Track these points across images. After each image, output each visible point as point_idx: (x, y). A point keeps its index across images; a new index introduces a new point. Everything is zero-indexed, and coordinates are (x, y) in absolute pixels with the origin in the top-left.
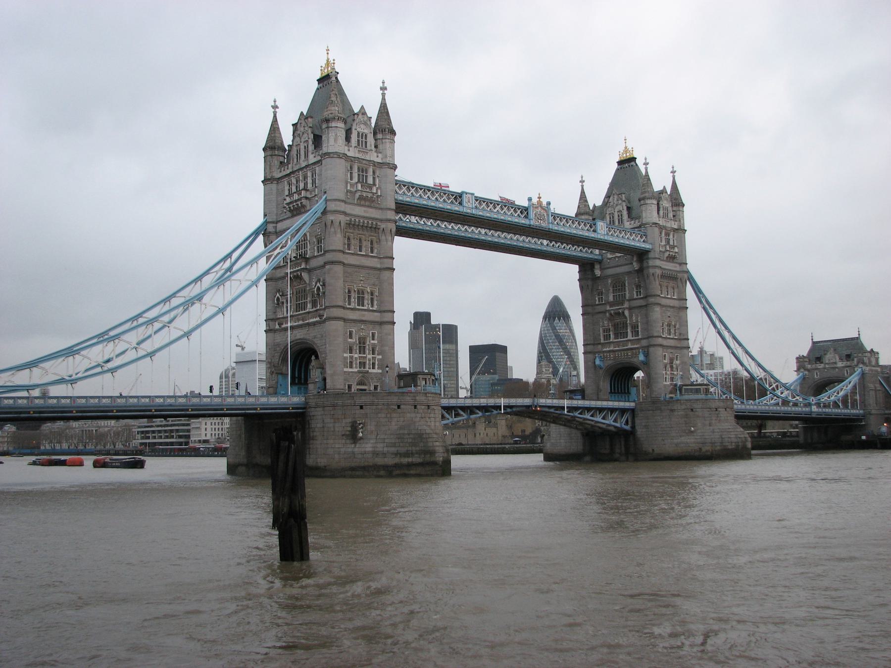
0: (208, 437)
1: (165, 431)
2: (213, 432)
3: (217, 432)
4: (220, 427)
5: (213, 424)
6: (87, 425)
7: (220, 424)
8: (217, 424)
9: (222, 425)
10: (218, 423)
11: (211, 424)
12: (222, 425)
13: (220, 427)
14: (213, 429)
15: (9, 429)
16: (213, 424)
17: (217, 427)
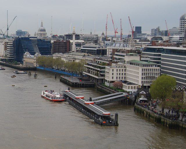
0: (114, 79)
1: (96, 70)
2: (118, 76)
3: (121, 76)
4: (124, 72)
5: (118, 70)
6: (70, 57)
7: (124, 70)
8: (121, 70)
9: (125, 71)
10: (122, 70)
11: (117, 71)
12: (125, 71)
13: (124, 72)
14: (118, 74)
15: (37, 55)
16: (118, 70)
17: (121, 72)
